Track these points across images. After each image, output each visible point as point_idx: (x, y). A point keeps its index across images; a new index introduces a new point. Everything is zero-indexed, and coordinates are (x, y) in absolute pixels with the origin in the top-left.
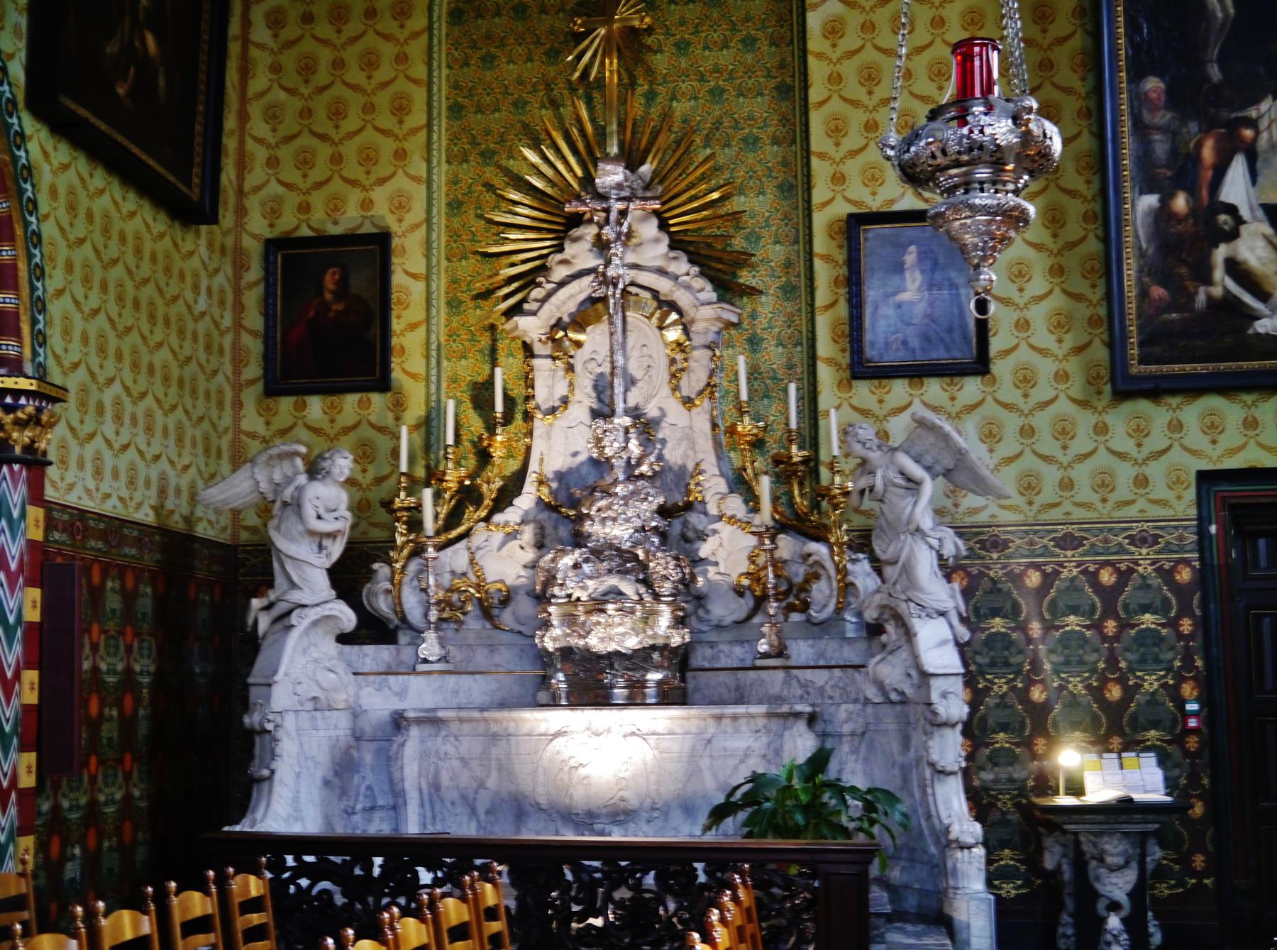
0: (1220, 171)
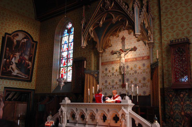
0: (12, 58)
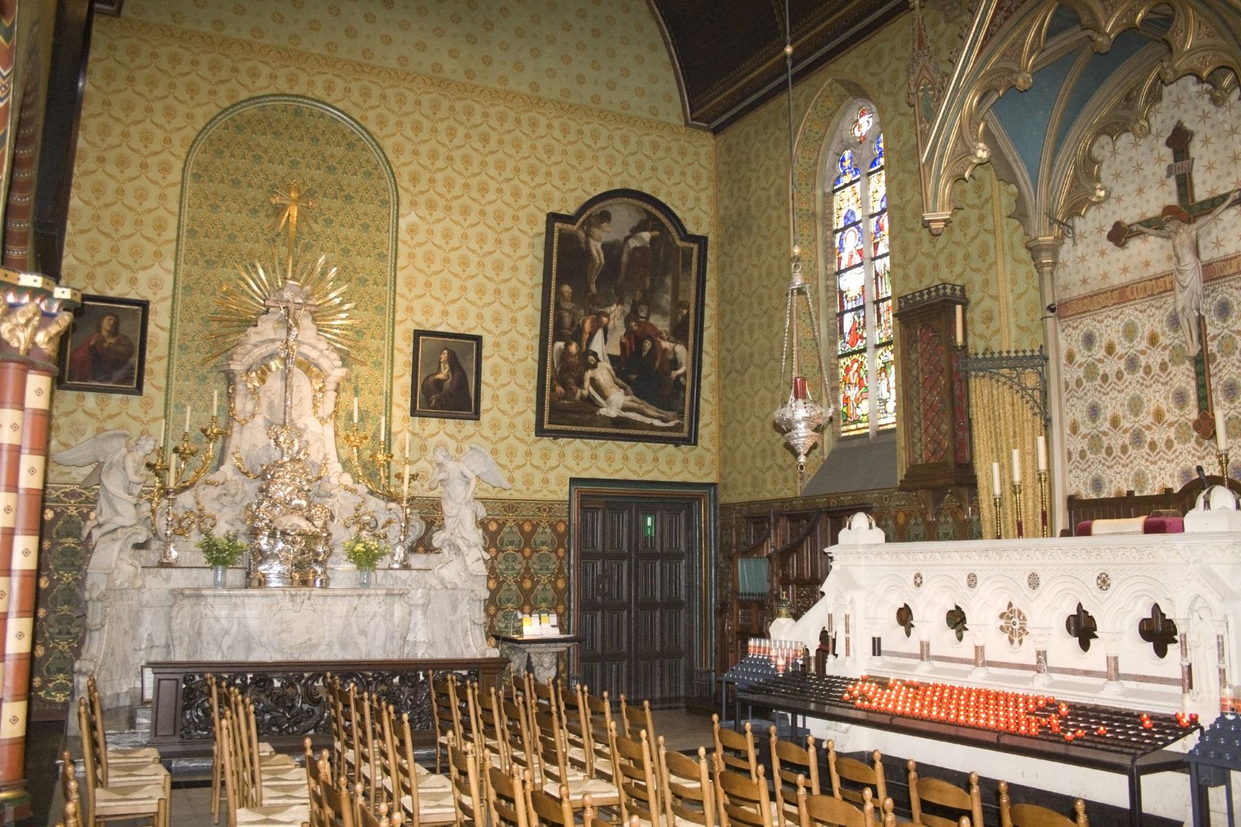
0: (592, 335)
